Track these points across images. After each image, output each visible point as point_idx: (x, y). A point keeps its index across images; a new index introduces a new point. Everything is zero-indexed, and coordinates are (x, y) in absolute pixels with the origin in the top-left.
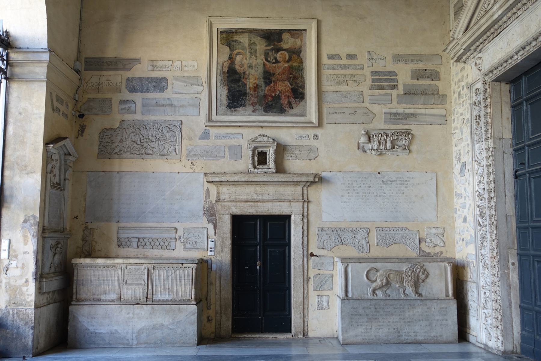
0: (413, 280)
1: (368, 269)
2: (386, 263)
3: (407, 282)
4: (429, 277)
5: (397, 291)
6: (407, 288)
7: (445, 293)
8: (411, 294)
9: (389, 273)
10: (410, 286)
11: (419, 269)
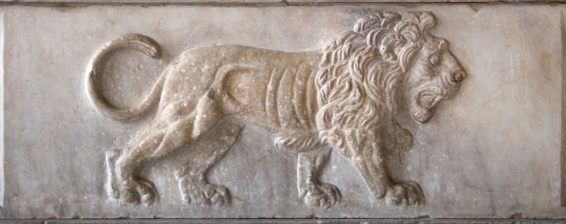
0: (369, 111)
1: (107, 44)
2: (214, 9)
3: (335, 117)
4: (469, 86)
5: (276, 174)
6: (337, 155)
7: (558, 184)
8: (356, 186)
9: (228, 67)
10: (349, 144)
11: (411, 44)
